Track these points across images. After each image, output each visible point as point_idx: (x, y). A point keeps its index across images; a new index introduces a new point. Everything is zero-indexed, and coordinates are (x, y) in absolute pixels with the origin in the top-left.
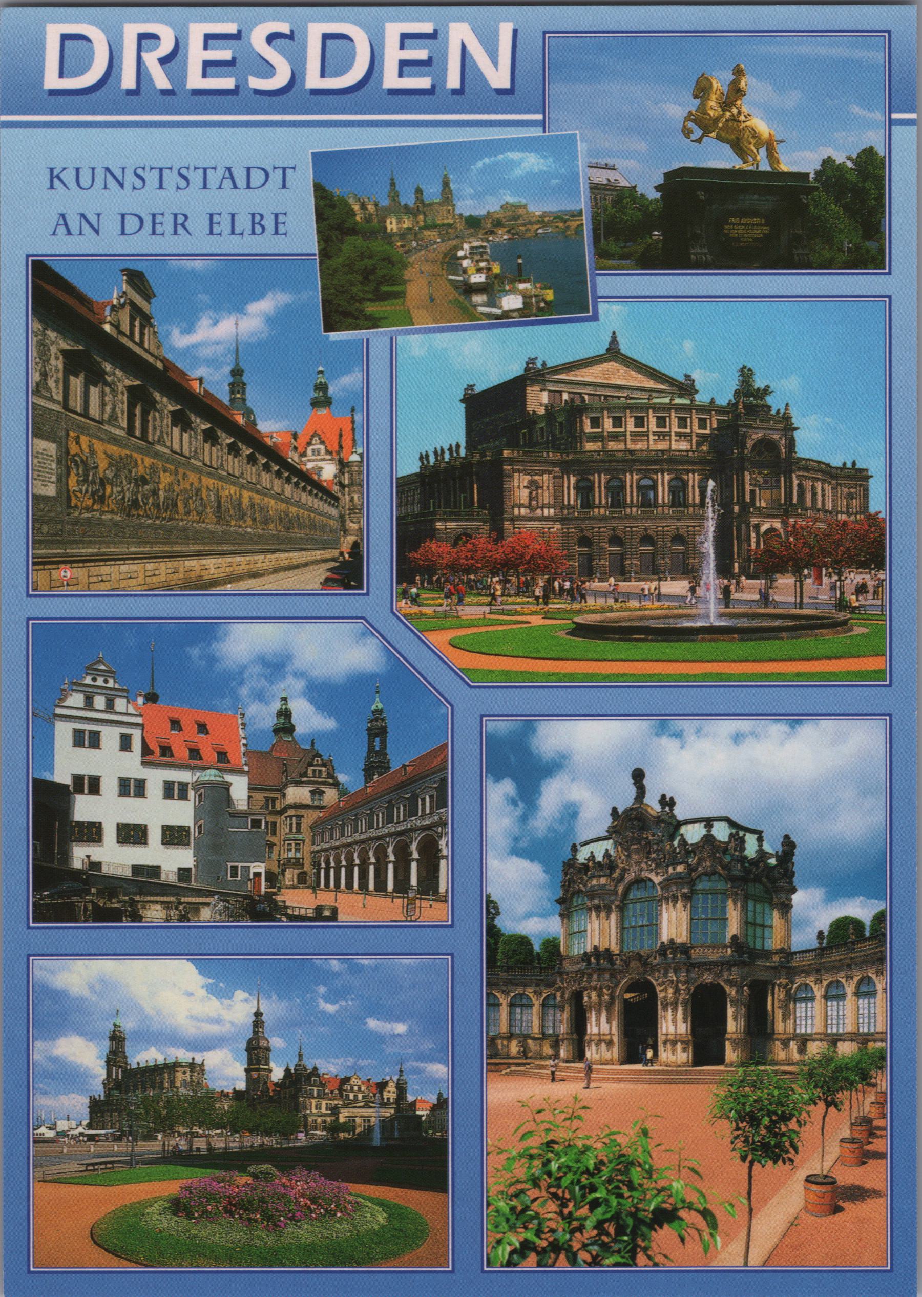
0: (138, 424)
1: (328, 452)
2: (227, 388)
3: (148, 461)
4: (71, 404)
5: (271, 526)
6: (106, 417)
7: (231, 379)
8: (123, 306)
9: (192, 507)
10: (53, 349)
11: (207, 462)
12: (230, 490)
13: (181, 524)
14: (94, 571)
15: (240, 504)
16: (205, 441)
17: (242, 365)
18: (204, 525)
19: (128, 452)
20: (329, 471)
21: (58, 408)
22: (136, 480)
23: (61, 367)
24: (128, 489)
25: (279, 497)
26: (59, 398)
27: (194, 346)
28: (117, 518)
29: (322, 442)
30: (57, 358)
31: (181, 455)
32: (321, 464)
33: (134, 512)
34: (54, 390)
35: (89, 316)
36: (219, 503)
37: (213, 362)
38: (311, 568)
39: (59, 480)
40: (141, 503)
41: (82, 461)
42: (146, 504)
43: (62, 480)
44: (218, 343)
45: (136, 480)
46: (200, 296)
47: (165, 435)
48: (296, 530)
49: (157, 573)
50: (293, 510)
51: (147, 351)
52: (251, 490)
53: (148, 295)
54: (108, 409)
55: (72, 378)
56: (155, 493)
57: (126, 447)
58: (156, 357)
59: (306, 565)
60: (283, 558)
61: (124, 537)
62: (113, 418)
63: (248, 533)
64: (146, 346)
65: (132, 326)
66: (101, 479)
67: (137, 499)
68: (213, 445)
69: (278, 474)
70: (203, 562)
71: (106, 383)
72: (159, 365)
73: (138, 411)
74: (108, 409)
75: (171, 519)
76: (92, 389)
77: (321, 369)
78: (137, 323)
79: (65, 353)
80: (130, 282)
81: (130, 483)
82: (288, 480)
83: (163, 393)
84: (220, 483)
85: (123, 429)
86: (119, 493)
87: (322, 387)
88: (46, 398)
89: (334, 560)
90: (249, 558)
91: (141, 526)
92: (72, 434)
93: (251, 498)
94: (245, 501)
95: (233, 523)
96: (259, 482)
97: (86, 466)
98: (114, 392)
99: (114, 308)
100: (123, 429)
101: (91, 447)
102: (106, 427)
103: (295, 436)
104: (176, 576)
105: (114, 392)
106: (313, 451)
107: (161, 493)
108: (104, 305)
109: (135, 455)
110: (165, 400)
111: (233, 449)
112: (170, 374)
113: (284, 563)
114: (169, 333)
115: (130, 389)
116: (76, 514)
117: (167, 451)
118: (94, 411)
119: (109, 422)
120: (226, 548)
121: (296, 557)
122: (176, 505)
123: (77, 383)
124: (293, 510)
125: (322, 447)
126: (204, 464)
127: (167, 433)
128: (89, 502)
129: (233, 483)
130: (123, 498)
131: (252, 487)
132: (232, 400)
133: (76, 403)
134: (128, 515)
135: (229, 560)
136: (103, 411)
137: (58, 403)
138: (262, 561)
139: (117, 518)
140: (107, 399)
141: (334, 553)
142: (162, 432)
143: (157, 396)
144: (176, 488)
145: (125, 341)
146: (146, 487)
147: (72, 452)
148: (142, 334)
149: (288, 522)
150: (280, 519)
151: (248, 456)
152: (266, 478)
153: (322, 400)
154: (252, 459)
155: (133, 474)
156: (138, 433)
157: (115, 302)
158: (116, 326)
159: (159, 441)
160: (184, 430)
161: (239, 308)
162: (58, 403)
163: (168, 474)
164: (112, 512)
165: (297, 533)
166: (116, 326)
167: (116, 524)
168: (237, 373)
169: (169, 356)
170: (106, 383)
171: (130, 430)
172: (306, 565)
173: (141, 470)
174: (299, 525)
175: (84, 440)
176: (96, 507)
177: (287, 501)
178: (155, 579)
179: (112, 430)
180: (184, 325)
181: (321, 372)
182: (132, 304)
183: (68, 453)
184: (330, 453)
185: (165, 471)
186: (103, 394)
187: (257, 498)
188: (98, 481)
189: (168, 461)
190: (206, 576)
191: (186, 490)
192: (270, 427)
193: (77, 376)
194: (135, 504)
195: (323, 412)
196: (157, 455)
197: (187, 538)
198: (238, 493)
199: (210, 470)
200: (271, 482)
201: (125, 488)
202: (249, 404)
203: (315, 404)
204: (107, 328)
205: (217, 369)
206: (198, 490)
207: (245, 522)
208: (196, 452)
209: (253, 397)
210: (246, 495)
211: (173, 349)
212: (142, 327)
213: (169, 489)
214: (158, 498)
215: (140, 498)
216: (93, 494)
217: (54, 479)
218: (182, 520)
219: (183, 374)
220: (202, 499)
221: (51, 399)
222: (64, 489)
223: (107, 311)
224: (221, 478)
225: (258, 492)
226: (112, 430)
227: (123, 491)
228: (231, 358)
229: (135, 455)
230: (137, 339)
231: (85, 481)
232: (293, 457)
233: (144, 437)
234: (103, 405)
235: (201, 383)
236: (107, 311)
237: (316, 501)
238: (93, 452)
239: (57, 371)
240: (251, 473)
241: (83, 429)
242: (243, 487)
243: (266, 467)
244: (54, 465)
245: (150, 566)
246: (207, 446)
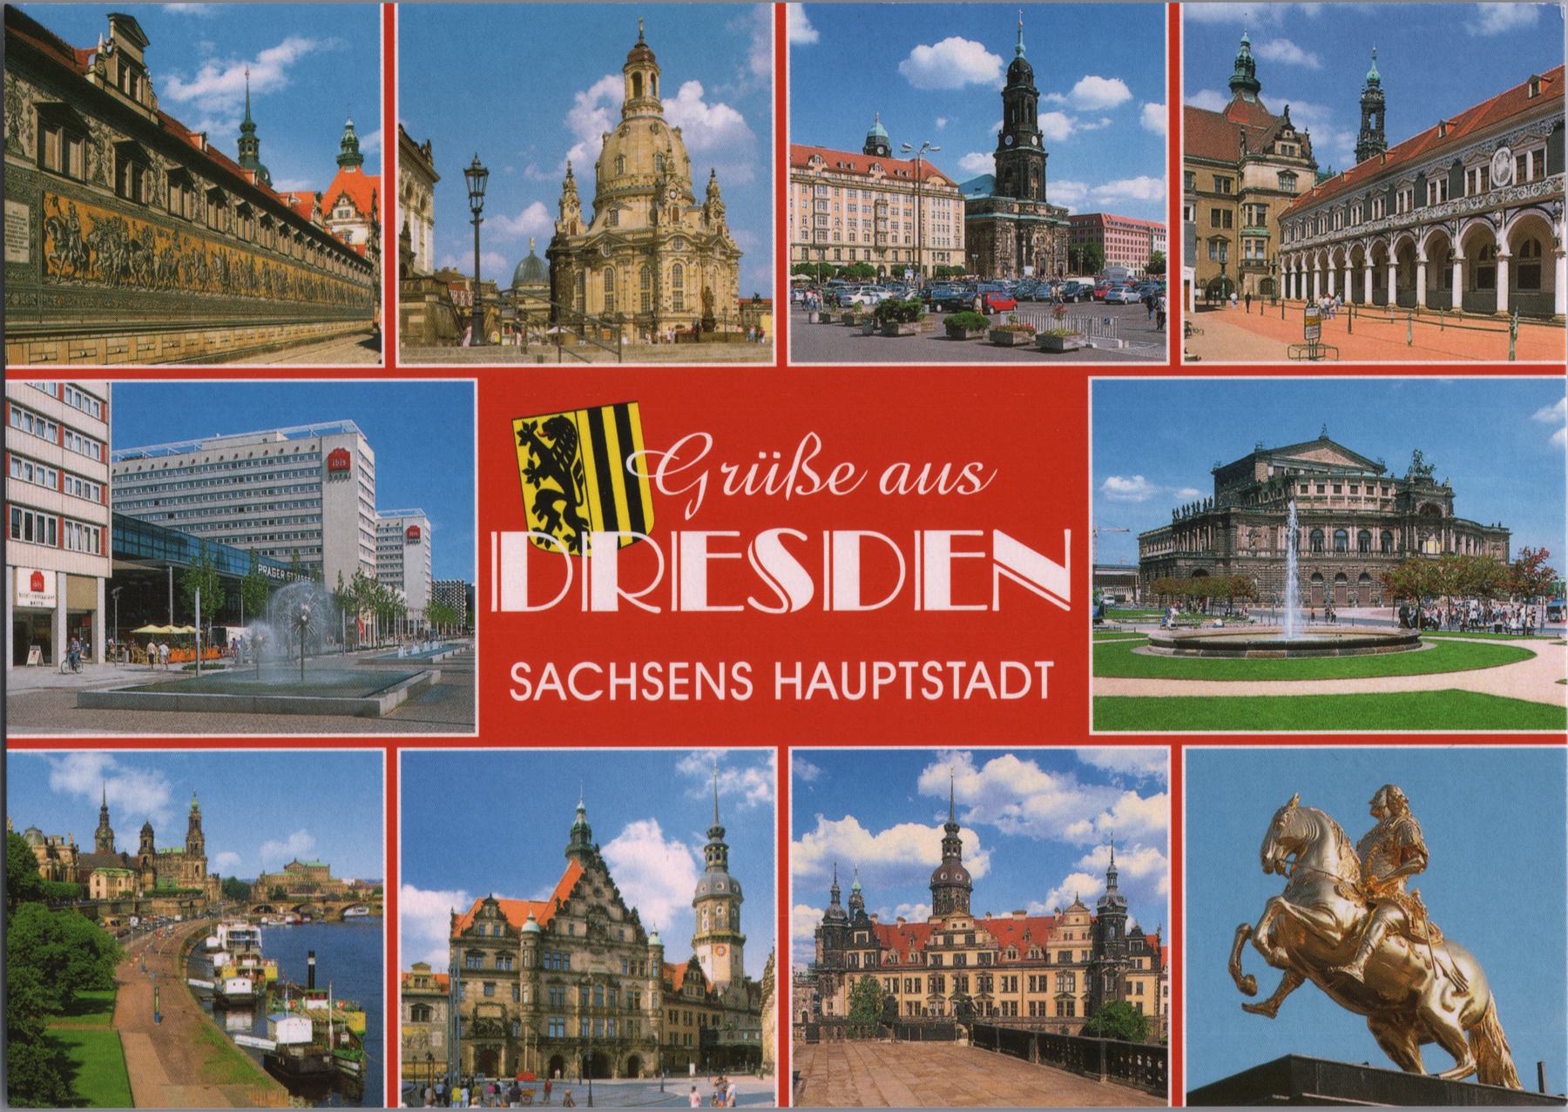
0: (128, 183)
1: (358, 214)
2: (236, 144)
3: (140, 225)
4: (48, 163)
5: (291, 295)
6: (90, 176)
7: (240, 135)
8: (110, 55)
10: (26, 102)
11: (212, 224)
12: (238, 257)
14: (76, 344)
15: (252, 269)
16: (210, 202)
17: (254, 119)
20: (359, 235)
21: (30, 166)
23: (34, 121)
25: (300, 263)
26: (34, 155)
27: (195, 99)
29: (352, 203)
30: (30, 112)
32: (350, 227)
33: (122, 280)
34: (27, 149)
35: (71, 65)
36: (227, 270)
37: (218, 116)
38: (339, 341)
39: (32, 246)
41: (61, 224)
42: (138, 272)
43: (36, 245)
44: (223, 95)
46: (203, 43)
50: (316, 277)
51: (141, 105)
52: (265, 255)
53: (140, 42)
54: (93, 168)
55: (48, 134)
56: (149, 259)
58: (150, 112)
59: (331, 338)
60: (305, 331)
62: (99, 176)
63: (260, 303)
64: (138, 98)
65: (121, 77)
66: (84, 245)
68: (219, 207)
69: (298, 239)
70: (207, 335)
71: (89, 139)
72: (154, 120)
73: (128, 170)
74: (93, 168)
75: (167, 288)
76: (73, 146)
77: (349, 123)
78: (127, 73)
79: (41, 107)
80: (118, 28)
82: (311, 245)
83: (158, 150)
85: (110, 189)
87: (352, 144)
88: (17, 156)
89: (367, 332)
90: (263, 330)
91: (132, 296)
92: (49, 196)
93: (265, 265)
94: (259, 266)
96: (274, 248)
97: (65, 231)
98: (100, 149)
99: (99, 57)
101: (72, 209)
102: (90, 187)
103: (319, 197)
104: (175, 351)
105: (100, 149)
106: (341, 214)
108: (88, 54)
109: (125, 218)
110: (161, 158)
111: (244, 212)
113: (305, 335)
114: (166, 83)
115: (118, 146)
116: (54, 282)
117: (164, 213)
118: (75, 168)
119: (94, 182)
120: (234, 318)
121: (319, 329)
123: (53, 140)
124: (316, 277)
125: (351, 209)
128: (71, 270)
129: (243, 248)
131: (266, 251)
132: (242, 158)
133: (54, 161)
134: (117, 283)
135: (238, 332)
136: (86, 169)
137: (32, 161)
138: (276, 334)
140: (91, 157)
141: (369, 324)
142: (157, 194)
143: (151, 153)
144: (177, 255)
145: (113, 93)
147: (49, 214)
148: (133, 86)
150: (301, 288)
151: (262, 219)
152: (284, 244)
153: (351, 156)
154: (266, 222)
157: (100, 50)
158: (102, 76)
160: (185, 190)
161: (249, 53)
162: (32, 161)
164: (98, 280)
166: (102, 76)
167: (102, 294)
168: (248, 128)
169: (166, 110)
170: (89, 139)
171: (120, 190)
172: (331, 338)
173: (132, 234)
174: (324, 295)
175: (63, 203)
176: (77, 275)
177: (309, 268)
179: (97, 190)
180: (185, 76)
181: (351, 127)
182: (122, 53)
183: (44, 215)
184: (362, 216)
185: (161, 235)
186: (86, 152)
187: (272, 264)
188: (80, 247)
189: (165, 224)
190: (210, 350)
191: (187, 256)
192: (288, 185)
193: (54, 132)
194: (125, 271)
195: (351, 170)
196: (153, 218)
197: (188, 307)
199: (218, 235)
200: (290, 247)
202: (262, 161)
203: (342, 162)
204: (91, 78)
205: (224, 122)
206: (202, 257)
208: (198, 214)
209: (266, 155)
210: (259, 261)
211: (170, 102)
212: (133, 78)
216: (74, 261)
217: (26, 244)
219: (183, 129)
221: (23, 157)
222: (39, 257)
223: (92, 60)
224: (228, 243)
225: (274, 258)
226: (97, 190)
228: (240, 111)
229: (125, 218)
230: (127, 91)
231: (65, 246)
232: (315, 220)
233: (136, 197)
234: (87, 163)
236: (92, 60)
237: (344, 268)
238: (74, 216)
239: (30, 126)
240: (264, 237)
241: (64, 191)
242: (256, 252)
243: (284, 231)
244: (27, 229)
245: (142, 339)
246: (212, 208)
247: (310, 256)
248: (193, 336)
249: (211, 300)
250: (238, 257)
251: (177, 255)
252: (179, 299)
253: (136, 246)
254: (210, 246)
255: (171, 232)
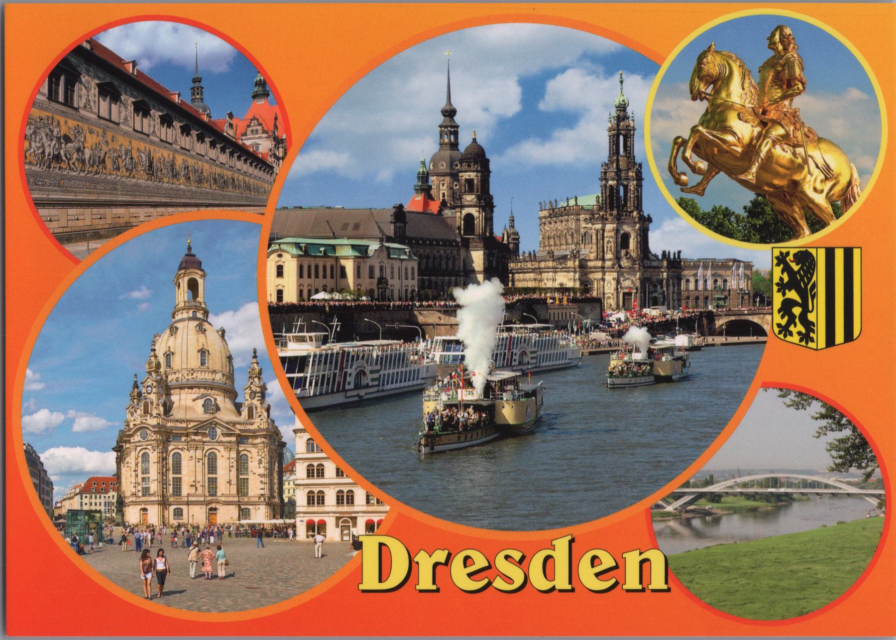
3: (72, 123)
9: (122, 165)
13: (109, 177)
15: (173, 166)
18: (134, 180)
19: (49, 115)
22: (58, 139)
24: (50, 145)
28: (37, 168)
31: (110, 121)
36: (151, 163)
40: (64, 158)
45: (58, 139)
47: (92, 104)
48: (230, 189)
49: (81, 217)
50: (228, 174)
57: (46, 109)
61: (43, 185)
67: (59, 153)
75: (96, 173)
81: (51, 140)
84: (152, 148)
86: (39, 148)
95: (165, 180)
100: (43, 94)
104: (102, 222)
107: (86, 150)
109: (57, 117)
112: (96, 52)
117: (94, 116)
122: (104, 161)
126: (134, 130)
127: (95, 102)
130: (43, 152)
139: (37, 168)
144: (105, 148)
146: (69, 145)
149: (222, 183)
150: (215, 180)
155: (55, 133)
156: (61, 99)
159: (85, 107)
163: (95, 136)
164: (30, 163)
165: (230, 192)
173: (64, 130)
174: (234, 187)
178: (80, 224)
185: (91, 132)
191: (115, 151)
194: (57, 158)
196: (83, 119)
197: (115, 189)
198: (171, 157)
201: (46, 145)
207: (178, 180)
213: (96, 147)
214: (83, 154)
215: (62, 153)
218: (110, 174)
220: (132, 158)
224: (152, 143)
225: (192, 157)
227: (43, 146)
229: (57, 117)
233: (68, 102)
235: (134, 67)
245: (72, 211)
247: (224, 158)
248: (121, 211)
249: (137, 185)
250: (161, 154)
251: (105, 148)
252: (106, 182)
253: (67, 139)
254: (135, 144)
255: (101, 131)
